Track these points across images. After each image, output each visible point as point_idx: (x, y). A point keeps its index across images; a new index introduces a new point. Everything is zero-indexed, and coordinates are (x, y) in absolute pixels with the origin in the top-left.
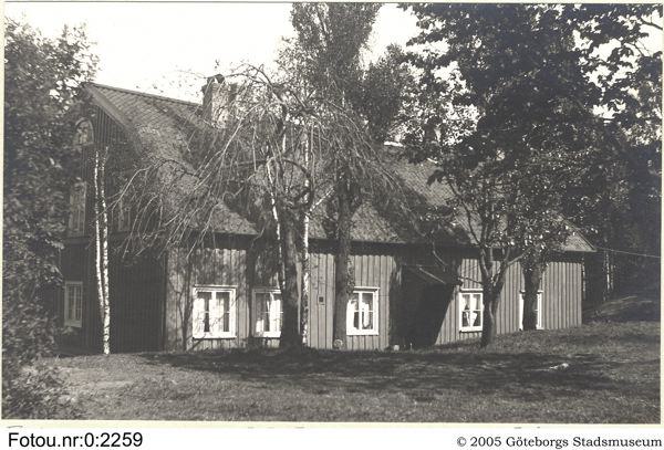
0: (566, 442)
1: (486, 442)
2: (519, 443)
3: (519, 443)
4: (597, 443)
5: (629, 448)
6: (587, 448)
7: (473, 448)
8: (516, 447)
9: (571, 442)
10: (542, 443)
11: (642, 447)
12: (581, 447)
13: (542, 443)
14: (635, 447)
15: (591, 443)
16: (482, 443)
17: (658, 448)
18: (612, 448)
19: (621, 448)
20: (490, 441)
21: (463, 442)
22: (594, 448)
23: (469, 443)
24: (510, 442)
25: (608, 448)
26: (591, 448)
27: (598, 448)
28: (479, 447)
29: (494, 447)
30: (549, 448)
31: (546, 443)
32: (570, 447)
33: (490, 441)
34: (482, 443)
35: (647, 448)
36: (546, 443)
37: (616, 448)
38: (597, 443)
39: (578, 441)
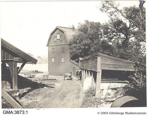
0: (123, 113)
1: (104, 113)
3: (112, 113)
5: (138, 114)
6: (128, 114)
7: (102, 114)
8: (112, 114)
9: (125, 113)
11: (141, 114)
12: (127, 114)
14: (140, 114)
15: (129, 113)
16: (104, 113)
17: (145, 114)
18: (134, 114)
19: (136, 114)
20: (104, 113)
21: (99, 113)
22: (130, 114)
25: (133, 114)
26: (129, 114)
27: (131, 114)
28: (103, 114)
29: (106, 114)
30: (119, 114)
31: (119, 113)
32: (124, 114)
33: (104, 113)
34: (104, 113)
35: (143, 114)
36: (119, 113)
37: (135, 114)
38: (131, 113)
39: (126, 113)
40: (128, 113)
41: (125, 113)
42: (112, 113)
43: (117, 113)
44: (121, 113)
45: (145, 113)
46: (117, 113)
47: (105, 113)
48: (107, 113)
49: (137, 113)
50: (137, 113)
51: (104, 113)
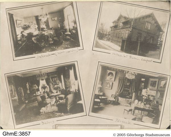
1: (121, 135)
2: (131, 135)
3: (131, 135)
4: (152, 135)
9: (145, 135)
10: (137, 135)
13: (137, 135)
15: (150, 135)
16: (120, 135)
20: (122, 134)
23: (117, 135)
24: (128, 135)
31: (138, 135)
33: (122, 134)
34: (120, 135)
36: (138, 135)
38: (152, 135)
39: (147, 135)
40: (149, 135)
41: (145, 135)
42: (130, 134)
43: (136, 135)
44: (140, 135)
45: (169, 135)
46: (136, 135)
47: (122, 135)
48: (125, 135)
49: (166, 135)
50: (159, 135)
51: (120, 135)
